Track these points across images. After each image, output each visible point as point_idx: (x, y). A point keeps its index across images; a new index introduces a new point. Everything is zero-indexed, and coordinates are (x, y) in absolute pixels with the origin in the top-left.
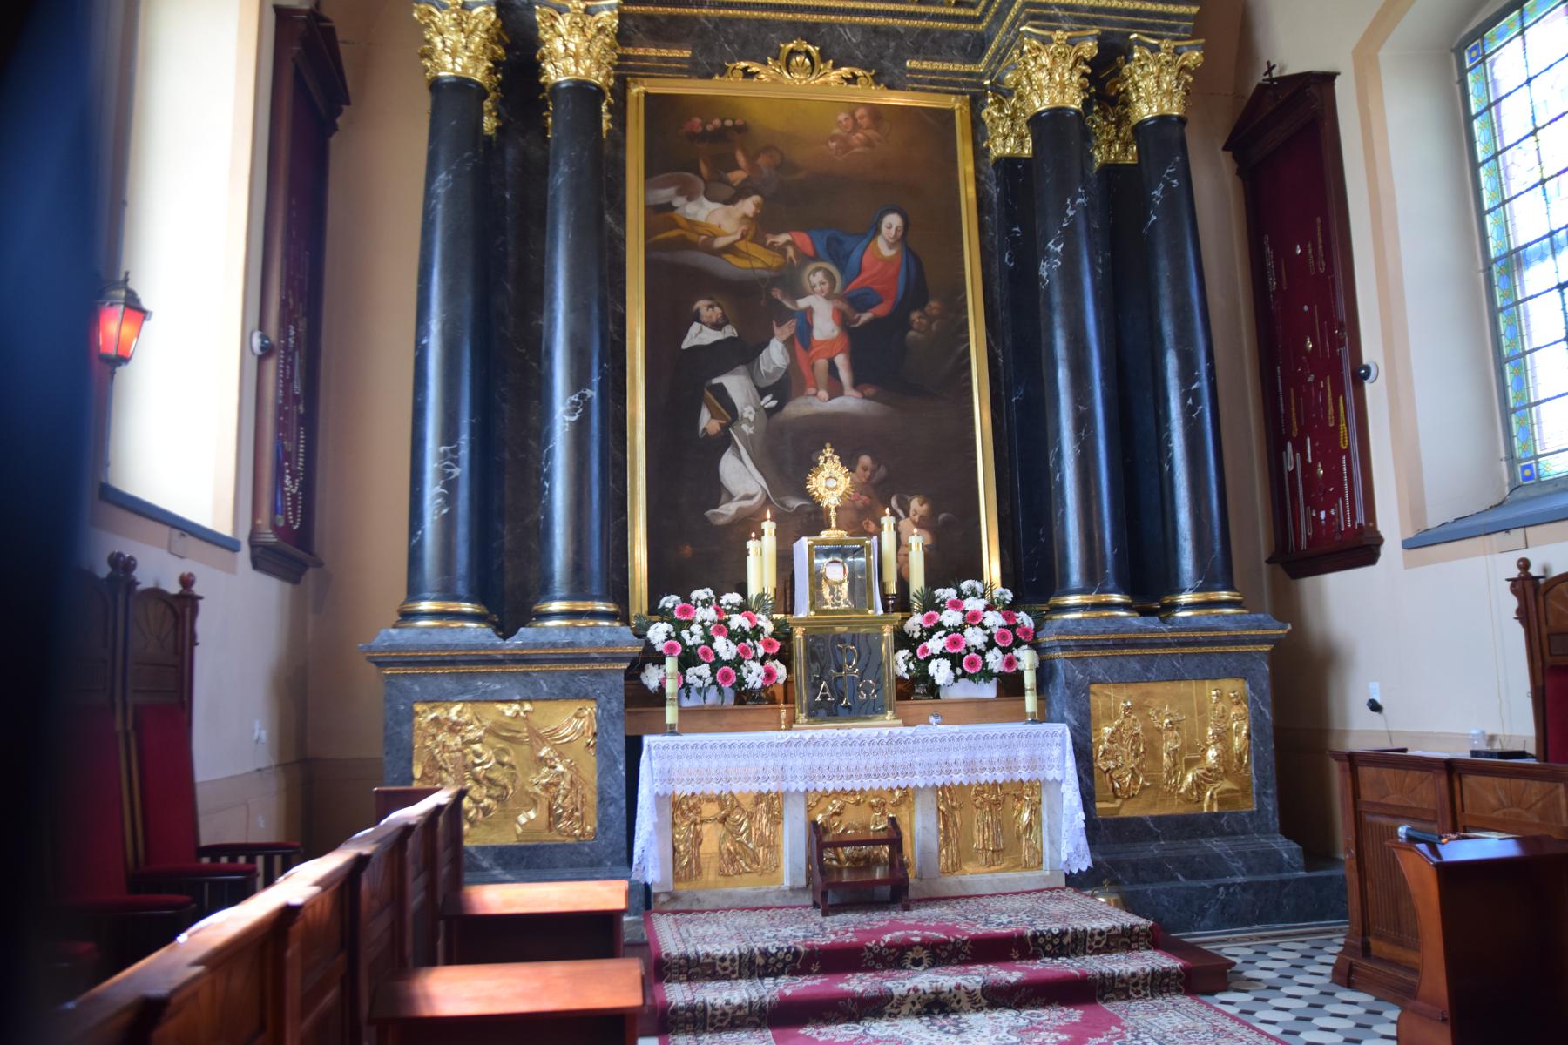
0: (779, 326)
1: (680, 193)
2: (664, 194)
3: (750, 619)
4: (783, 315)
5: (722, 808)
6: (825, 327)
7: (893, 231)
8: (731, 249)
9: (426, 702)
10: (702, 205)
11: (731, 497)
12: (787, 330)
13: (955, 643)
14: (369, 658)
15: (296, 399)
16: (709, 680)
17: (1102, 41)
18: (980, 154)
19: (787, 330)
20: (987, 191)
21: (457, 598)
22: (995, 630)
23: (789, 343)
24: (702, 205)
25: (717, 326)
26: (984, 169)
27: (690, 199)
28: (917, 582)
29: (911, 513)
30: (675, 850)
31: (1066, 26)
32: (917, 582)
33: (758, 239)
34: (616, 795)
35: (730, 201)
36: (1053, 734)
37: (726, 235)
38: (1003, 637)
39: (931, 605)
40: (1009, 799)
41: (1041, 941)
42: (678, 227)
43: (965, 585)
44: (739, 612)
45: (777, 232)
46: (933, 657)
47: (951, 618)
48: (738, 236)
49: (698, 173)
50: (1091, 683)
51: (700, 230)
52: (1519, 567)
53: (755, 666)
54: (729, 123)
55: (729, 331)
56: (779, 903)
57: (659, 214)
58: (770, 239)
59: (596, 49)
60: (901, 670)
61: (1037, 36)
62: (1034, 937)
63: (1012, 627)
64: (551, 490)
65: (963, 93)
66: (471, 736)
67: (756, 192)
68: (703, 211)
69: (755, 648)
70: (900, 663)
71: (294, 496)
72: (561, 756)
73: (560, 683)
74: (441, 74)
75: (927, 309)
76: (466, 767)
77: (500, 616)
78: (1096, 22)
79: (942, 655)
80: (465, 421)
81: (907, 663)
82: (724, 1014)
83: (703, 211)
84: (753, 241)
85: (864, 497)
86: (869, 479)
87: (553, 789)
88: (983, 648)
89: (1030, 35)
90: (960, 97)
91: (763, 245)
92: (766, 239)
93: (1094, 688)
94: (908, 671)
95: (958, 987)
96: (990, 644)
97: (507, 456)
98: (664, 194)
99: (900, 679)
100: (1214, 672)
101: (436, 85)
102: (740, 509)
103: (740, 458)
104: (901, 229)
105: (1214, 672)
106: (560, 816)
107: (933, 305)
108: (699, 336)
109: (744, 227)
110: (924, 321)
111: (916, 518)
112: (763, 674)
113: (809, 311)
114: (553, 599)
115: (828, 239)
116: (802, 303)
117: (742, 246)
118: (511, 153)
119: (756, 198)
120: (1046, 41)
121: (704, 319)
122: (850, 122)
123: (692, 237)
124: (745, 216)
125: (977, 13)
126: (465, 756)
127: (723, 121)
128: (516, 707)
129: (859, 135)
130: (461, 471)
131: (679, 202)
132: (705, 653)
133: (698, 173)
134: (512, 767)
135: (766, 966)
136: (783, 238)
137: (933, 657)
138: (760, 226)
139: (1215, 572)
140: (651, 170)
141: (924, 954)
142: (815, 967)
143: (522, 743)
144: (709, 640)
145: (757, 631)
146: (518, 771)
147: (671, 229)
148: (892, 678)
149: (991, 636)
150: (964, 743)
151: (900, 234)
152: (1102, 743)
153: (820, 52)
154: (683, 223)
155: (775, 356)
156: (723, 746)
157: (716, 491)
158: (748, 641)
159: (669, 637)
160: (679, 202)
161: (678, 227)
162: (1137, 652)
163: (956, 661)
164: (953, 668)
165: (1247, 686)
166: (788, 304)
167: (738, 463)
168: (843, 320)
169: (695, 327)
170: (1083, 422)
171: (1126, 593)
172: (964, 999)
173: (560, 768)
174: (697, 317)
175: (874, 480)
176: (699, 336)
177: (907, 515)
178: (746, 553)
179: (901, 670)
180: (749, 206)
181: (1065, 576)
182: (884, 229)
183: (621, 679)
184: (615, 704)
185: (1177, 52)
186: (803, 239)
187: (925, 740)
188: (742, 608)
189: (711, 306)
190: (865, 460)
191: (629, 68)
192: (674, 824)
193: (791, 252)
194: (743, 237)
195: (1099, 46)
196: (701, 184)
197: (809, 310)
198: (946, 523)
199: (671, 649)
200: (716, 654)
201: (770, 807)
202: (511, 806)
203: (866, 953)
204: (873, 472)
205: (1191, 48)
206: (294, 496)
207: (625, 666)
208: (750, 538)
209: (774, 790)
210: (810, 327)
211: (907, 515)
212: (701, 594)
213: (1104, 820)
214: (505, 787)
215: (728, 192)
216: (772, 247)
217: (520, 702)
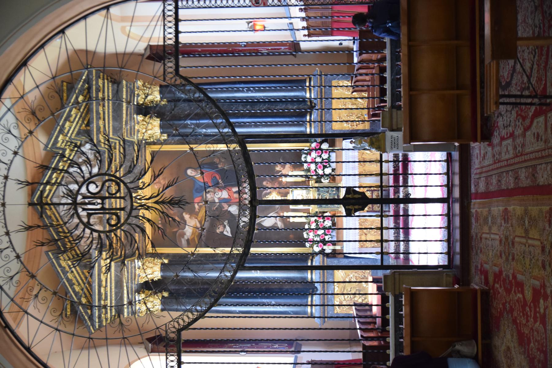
0: (224, 208)
1: (183, 237)
2: (184, 242)
3: (313, 223)
4: (221, 207)
5: (363, 235)
6: (224, 194)
7: (193, 172)
8: (200, 222)
9: (334, 310)
10: (187, 231)
11: (276, 223)
12: (225, 206)
13: (320, 167)
14: (323, 325)
15: (252, 345)
16: (330, 236)
17: (138, 114)
18: (165, 142)
19: (225, 206)
20: (177, 140)
21: (307, 302)
22: (317, 155)
23: (229, 206)
24: (187, 231)
25: (225, 227)
26: (170, 141)
27: (185, 234)
28: (302, 173)
29: (280, 170)
30: (373, 247)
31: (133, 124)
32: (302, 173)
33: (197, 214)
34: (359, 261)
35: (185, 221)
36: (346, 145)
37: (196, 223)
38: (318, 153)
39: (308, 170)
40: (363, 156)
41: (395, 166)
42: (194, 238)
43: (303, 159)
44: (311, 226)
45: (195, 208)
46: (324, 172)
47: (313, 167)
48: (196, 220)
49: (176, 232)
50: (332, 129)
51: (195, 231)
52: (303, 20)
53: (326, 222)
54: (160, 222)
55: (226, 223)
56: (388, 221)
57: (189, 243)
58: (197, 210)
59: (151, 265)
60: (327, 181)
61: (137, 134)
62: (394, 167)
63: (316, 150)
64: (278, 277)
65: (145, 147)
66: (343, 299)
67: (182, 214)
68: (188, 231)
69: (320, 222)
70: (325, 181)
71: (279, 345)
72: (349, 275)
73: (330, 276)
74: (160, 309)
75: (217, 162)
76: (351, 300)
77: (310, 289)
78: (131, 114)
79: (323, 170)
80: (259, 300)
81: (325, 179)
82: (405, 246)
83: (188, 231)
84: (198, 215)
85: (276, 184)
86: (270, 182)
87: (357, 278)
88: (321, 158)
89: (137, 136)
90: (147, 149)
91: (199, 212)
92: (197, 212)
93: (333, 128)
94: (327, 179)
95: (403, 192)
96: (320, 156)
97: (264, 287)
98: (184, 242)
99: (330, 182)
100: (330, 91)
101: (162, 310)
102: (279, 221)
103: (264, 220)
104: (192, 170)
105: (330, 91)
106: (364, 276)
107: (216, 160)
108: (228, 232)
109: (193, 218)
110: (221, 164)
111: (282, 168)
112: (328, 221)
113: (219, 198)
114: (307, 277)
115: (196, 192)
116: (217, 201)
117: (199, 219)
118: (172, 287)
119: (184, 214)
120: (138, 131)
121: (223, 230)
122: (158, 184)
123: (197, 234)
124: (190, 217)
125: (117, 142)
126: (348, 300)
127: (159, 224)
128: (336, 287)
129: (162, 181)
130: (273, 302)
131: (186, 237)
132: (322, 237)
133: (176, 232)
134: (351, 288)
135: (397, 233)
136: (196, 206)
137: (324, 172)
138: (193, 213)
139: (299, 83)
140: (177, 246)
141: (397, 195)
142: (398, 221)
143: (345, 285)
144: (319, 235)
145: (316, 221)
146: (352, 286)
147: (195, 240)
148: (329, 184)
149: (318, 156)
150: (348, 170)
151: (194, 170)
152: (349, 126)
153: (135, 193)
154: (193, 236)
155: (234, 209)
156: (347, 235)
157: (274, 228)
158: (319, 224)
159: (318, 246)
160: (186, 237)
161: (194, 238)
162: (324, 115)
163: (325, 167)
164: (327, 167)
165: (334, 81)
166: (218, 204)
167: (266, 221)
168: (221, 189)
169: (225, 233)
170: (256, 125)
171: (306, 116)
172: (405, 190)
173: (352, 276)
174: (222, 232)
175: (271, 181)
176: (228, 232)
177: (281, 171)
178: (293, 222)
179: (327, 181)
180: (186, 216)
181: (302, 131)
182: (192, 175)
183: (329, 260)
184: (335, 262)
185: (138, 88)
186: (197, 200)
187: (346, 181)
188: (309, 224)
189: (219, 228)
190: (264, 183)
191: (143, 252)
192: (367, 247)
193: (200, 204)
194: (197, 218)
195: (139, 114)
196: (180, 231)
197: (219, 198)
198: (283, 159)
199: (321, 246)
200: (322, 234)
201: (364, 222)
202: (361, 288)
203: (396, 209)
204: (268, 181)
205: (137, 84)
206: (279, 345)
207: (325, 259)
208: (289, 221)
209: (359, 221)
210: (224, 199)
211: (281, 171)
212: (305, 236)
213: (371, 127)
214: (357, 290)
215: (182, 222)
216: (199, 210)
217: (334, 286)
